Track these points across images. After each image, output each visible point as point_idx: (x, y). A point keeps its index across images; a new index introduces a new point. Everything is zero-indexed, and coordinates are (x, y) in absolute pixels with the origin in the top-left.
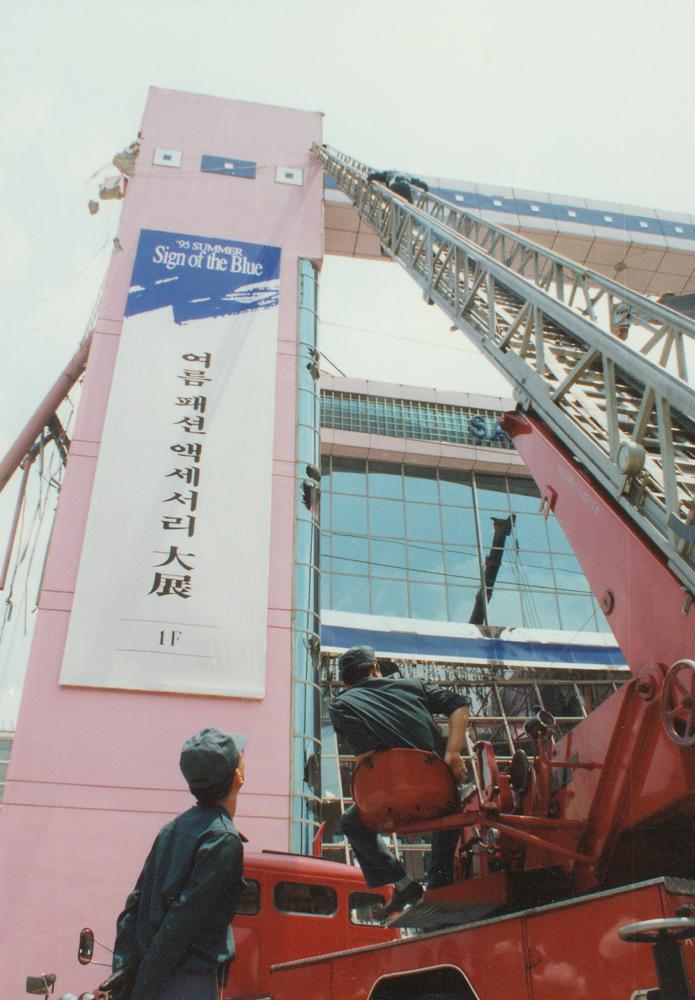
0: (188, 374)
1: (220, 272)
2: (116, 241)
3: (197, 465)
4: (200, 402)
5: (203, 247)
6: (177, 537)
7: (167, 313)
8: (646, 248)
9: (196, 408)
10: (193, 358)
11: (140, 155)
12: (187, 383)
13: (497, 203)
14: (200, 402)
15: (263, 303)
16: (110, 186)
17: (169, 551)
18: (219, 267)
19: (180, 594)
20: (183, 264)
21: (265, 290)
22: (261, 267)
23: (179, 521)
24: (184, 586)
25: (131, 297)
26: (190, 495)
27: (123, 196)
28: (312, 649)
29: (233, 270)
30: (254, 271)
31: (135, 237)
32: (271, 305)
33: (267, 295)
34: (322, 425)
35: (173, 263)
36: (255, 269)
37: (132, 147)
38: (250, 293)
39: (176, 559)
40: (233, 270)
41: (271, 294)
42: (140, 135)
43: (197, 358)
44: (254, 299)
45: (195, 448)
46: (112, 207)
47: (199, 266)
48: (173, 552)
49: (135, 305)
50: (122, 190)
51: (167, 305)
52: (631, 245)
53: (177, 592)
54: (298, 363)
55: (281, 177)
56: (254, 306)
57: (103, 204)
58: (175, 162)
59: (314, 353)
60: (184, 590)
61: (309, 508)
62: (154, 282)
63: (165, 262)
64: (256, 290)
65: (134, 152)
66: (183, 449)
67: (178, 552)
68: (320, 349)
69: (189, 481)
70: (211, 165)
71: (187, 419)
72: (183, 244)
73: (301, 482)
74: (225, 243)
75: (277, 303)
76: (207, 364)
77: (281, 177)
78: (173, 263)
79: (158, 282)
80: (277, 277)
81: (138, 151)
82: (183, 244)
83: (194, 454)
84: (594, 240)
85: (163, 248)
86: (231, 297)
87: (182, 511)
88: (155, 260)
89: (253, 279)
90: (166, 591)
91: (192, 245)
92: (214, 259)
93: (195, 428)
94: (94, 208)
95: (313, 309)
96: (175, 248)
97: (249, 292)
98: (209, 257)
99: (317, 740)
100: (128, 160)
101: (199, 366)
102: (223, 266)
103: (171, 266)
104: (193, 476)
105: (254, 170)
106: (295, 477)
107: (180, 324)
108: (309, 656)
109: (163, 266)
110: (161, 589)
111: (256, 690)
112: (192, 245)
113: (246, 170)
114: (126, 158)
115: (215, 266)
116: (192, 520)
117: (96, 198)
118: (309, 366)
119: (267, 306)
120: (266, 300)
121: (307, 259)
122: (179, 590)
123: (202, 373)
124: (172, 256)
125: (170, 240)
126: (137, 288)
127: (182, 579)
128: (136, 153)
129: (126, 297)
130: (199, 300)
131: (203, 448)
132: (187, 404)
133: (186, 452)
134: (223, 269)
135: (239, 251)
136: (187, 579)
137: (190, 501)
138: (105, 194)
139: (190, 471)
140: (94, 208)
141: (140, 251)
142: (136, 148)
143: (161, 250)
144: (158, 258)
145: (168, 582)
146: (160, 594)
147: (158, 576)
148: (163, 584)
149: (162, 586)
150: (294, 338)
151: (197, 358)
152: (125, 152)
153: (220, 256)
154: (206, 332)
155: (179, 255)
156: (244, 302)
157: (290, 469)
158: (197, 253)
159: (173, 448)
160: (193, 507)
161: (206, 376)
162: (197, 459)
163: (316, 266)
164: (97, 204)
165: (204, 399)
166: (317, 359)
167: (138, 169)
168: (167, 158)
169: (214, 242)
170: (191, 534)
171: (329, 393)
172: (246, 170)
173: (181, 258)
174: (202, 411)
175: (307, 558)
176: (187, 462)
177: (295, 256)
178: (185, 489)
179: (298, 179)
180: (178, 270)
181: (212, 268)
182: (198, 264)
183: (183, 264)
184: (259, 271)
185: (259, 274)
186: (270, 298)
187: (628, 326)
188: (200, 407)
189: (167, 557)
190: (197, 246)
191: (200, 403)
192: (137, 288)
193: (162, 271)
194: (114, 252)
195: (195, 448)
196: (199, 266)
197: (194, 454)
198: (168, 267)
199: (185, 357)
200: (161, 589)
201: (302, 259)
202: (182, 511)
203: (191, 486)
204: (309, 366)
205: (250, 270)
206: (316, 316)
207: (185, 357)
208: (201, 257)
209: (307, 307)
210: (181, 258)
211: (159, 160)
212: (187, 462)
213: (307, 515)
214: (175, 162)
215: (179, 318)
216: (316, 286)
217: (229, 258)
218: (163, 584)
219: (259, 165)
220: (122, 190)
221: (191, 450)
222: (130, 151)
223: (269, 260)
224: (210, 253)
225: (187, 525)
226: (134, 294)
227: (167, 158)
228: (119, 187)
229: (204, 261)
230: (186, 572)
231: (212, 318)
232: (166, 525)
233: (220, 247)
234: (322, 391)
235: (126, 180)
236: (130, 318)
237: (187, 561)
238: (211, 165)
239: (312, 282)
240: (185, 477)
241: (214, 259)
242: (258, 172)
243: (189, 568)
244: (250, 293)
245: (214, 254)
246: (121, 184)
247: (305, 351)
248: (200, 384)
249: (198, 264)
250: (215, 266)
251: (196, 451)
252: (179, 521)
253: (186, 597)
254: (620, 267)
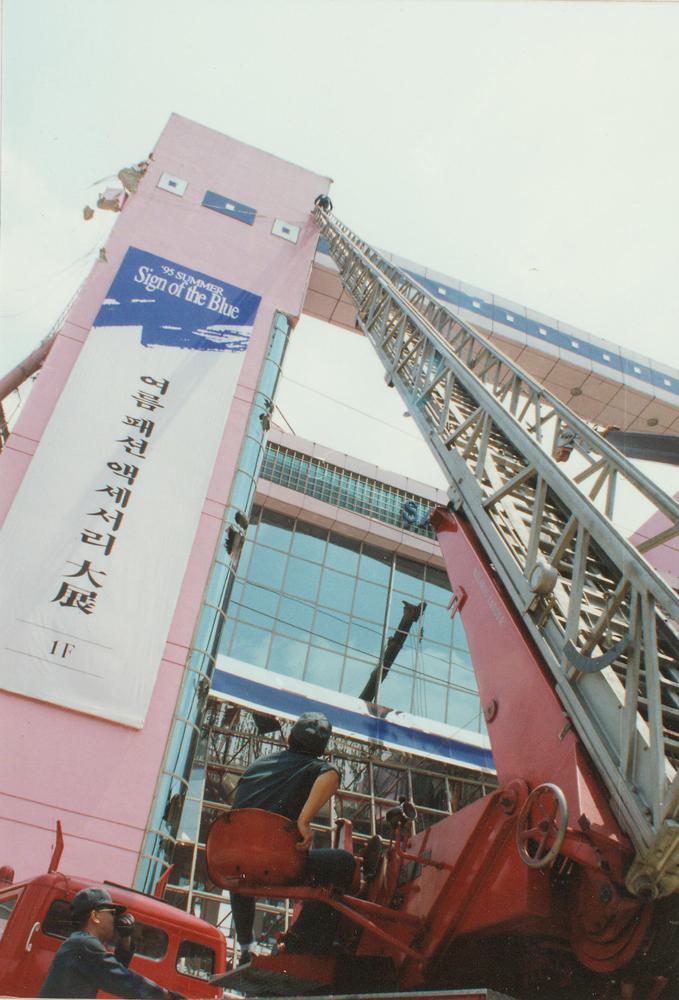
0: (142, 396)
1: (197, 305)
2: (103, 251)
3: (129, 487)
4: (147, 426)
5: (186, 278)
6: (93, 553)
7: (136, 331)
8: (603, 380)
9: (142, 431)
10: (150, 381)
11: (147, 175)
12: (139, 404)
13: (476, 305)
14: (147, 426)
15: (231, 346)
16: (109, 197)
17: (82, 564)
18: (197, 301)
19: (82, 608)
20: (163, 289)
21: (237, 334)
22: (238, 311)
23: (98, 537)
24: (88, 602)
25: (104, 308)
26: (115, 515)
27: (120, 210)
28: (201, 691)
29: (210, 307)
30: (230, 314)
31: (124, 251)
32: (238, 349)
33: (237, 339)
34: (261, 476)
35: (153, 286)
36: (232, 312)
37: (140, 165)
38: (222, 334)
39: (86, 573)
40: (210, 307)
41: (241, 339)
42: (151, 156)
43: (154, 383)
44: (223, 340)
45: (132, 470)
46: (107, 219)
47: (178, 295)
48: (86, 566)
49: (106, 317)
50: (120, 205)
51: (135, 323)
52: (590, 374)
53: (79, 606)
54: (250, 413)
55: (278, 230)
56: (222, 346)
57: (99, 213)
58: (180, 190)
59: (269, 405)
60: (87, 606)
61: (229, 553)
62: (130, 300)
63: (146, 283)
64: (227, 332)
65: (142, 170)
66: (119, 468)
67: (91, 567)
68: (276, 402)
69: (118, 501)
70: (213, 201)
71: (130, 440)
72: (167, 270)
73: (227, 526)
74: (208, 279)
75: (245, 349)
76: (163, 392)
77: (278, 230)
78: (153, 286)
79: (134, 301)
80: (251, 324)
81: (145, 170)
82: (167, 270)
83: (129, 475)
84: (558, 361)
85: (147, 269)
86: (201, 333)
87: (104, 528)
88: (136, 279)
89: (229, 321)
90: (69, 603)
91: (175, 273)
92: (194, 292)
93: (136, 450)
94: (88, 214)
95: (278, 363)
96: (159, 273)
97: (220, 332)
98: (190, 289)
99: (184, 781)
100: (133, 177)
101: (155, 391)
102: (202, 301)
103: (150, 288)
104: (123, 497)
105: (253, 217)
106: (223, 521)
107: (146, 346)
108: (196, 697)
109: (142, 286)
110: (64, 599)
111: (136, 719)
112: (175, 273)
113: (245, 215)
114: (133, 175)
115: (194, 298)
116: (112, 539)
117: (93, 206)
118: (261, 417)
120: (235, 343)
121: (283, 313)
122: (83, 604)
123: (156, 398)
124: (154, 279)
125: (156, 263)
127: (89, 594)
128: (143, 172)
129: (100, 307)
130: (170, 328)
131: (139, 472)
132: (134, 425)
133: (121, 472)
134: (200, 304)
135: (220, 290)
136: (93, 595)
137: (114, 521)
138: (103, 203)
139: (121, 491)
140: (88, 214)
141: (122, 269)
142: (144, 167)
143: (144, 270)
144: (139, 278)
145: (74, 594)
146: (62, 604)
147: (65, 586)
148: (68, 594)
149: (67, 597)
150: (253, 386)
151: (154, 383)
152: (133, 169)
153: (201, 290)
154: (168, 360)
155: (161, 280)
156: (214, 341)
157: (220, 510)
158: (179, 282)
159: (110, 465)
160: (116, 527)
161: (160, 402)
162: (131, 482)
163: (292, 323)
164: (92, 212)
165: (152, 424)
166: (271, 411)
167: (140, 188)
168: (172, 184)
169: (198, 275)
170: (107, 552)
171: (275, 446)
172: (245, 215)
173: (163, 283)
174: (148, 435)
175: (216, 600)
176: (120, 482)
177: (274, 308)
178: (113, 508)
179: (293, 236)
180: (156, 294)
181: (190, 300)
182: (178, 292)
183: (163, 289)
184: (235, 314)
185: (233, 317)
186: (239, 343)
187: (572, 449)
188: (146, 430)
189: (80, 569)
190: (180, 275)
191: (147, 427)
193: (140, 291)
194: (98, 262)
195: (132, 470)
196: (178, 295)
197: (129, 475)
198: (147, 288)
199: (143, 379)
200: (64, 599)
201: (278, 312)
202: (104, 528)
203: (119, 506)
204: (261, 417)
205: (227, 312)
206: (280, 371)
207: (143, 379)
208: (182, 286)
209: (272, 360)
210: (163, 283)
211: (164, 184)
212: (120, 482)
213: (226, 558)
214: (180, 190)
215: (147, 340)
216: (287, 341)
217: (209, 295)
218: (68, 594)
219: (258, 214)
220: (120, 205)
221: (127, 471)
222: (138, 169)
223: (247, 306)
224: (192, 285)
225: (106, 544)
226: (107, 306)
227: (172, 184)
228: (118, 200)
229: (184, 292)
230: (93, 589)
231: (178, 348)
232: (85, 539)
233: (203, 283)
234: (269, 443)
235: (127, 196)
236: (98, 328)
237: (98, 578)
238: (213, 201)
239: (284, 337)
240: (116, 496)
241: (194, 292)
242: (256, 219)
243: (97, 585)
244: (222, 334)
245: (195, 287)
246: (121, 198)
247: (261, 401)
248: (152, 408)
249: (178, 292)
250: (194, 298)
251: (131, 473)
252: (98, 537)
253: (88, 612)
254: (577, 392)
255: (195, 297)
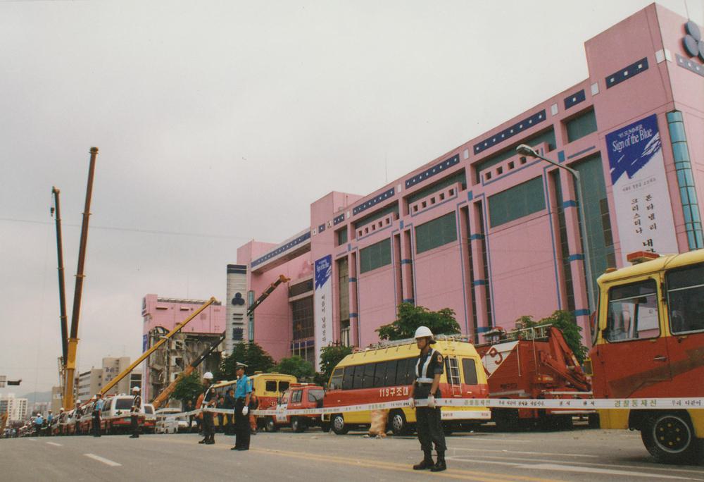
7: (625, 175)
21: (655, 142)
33: (655, 145)
36: (648, 134)
38: (650, 148)
44: (652, 149)
56: (653, 154)
64: (652, 144)
72: (621, 135)
82: (621, 135)
86: (644, 154)
89: (650, 138)
98: (632, 138)
109: (617, 151)
119: (657, 150)
126: (613, 169)
135: (641, 126)
153: (637, 133)
184: (651, 133)
190: (626, 133)
192: (613, 169)
215: (630, 175)
224: (631, 135)
244: (650, 148)
255: (635, 140)
